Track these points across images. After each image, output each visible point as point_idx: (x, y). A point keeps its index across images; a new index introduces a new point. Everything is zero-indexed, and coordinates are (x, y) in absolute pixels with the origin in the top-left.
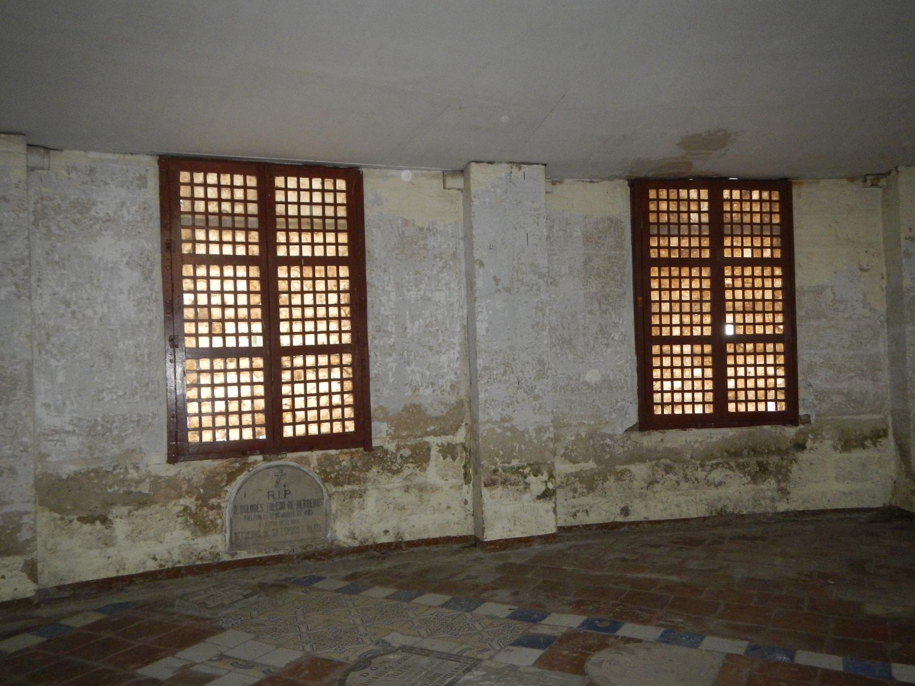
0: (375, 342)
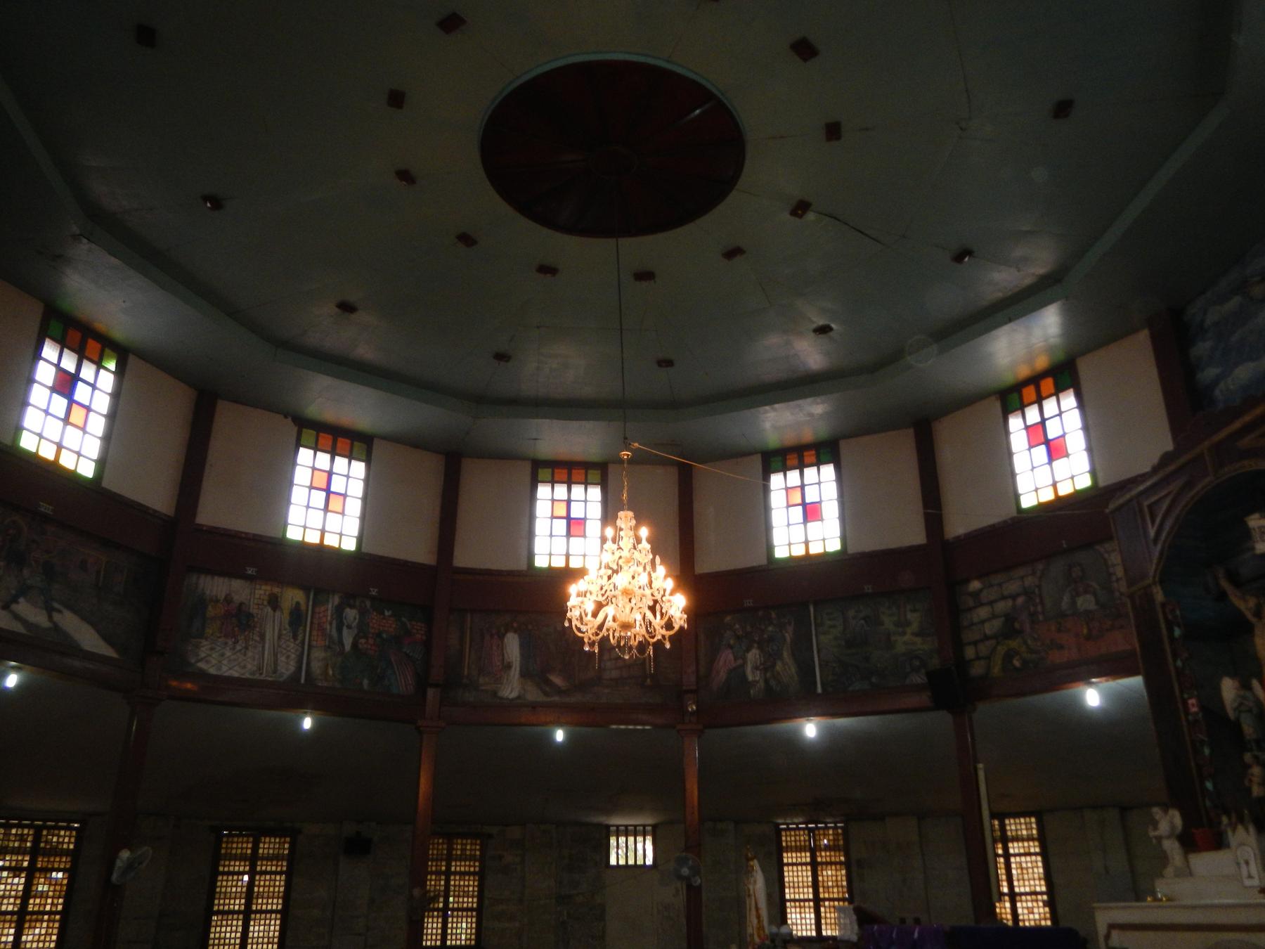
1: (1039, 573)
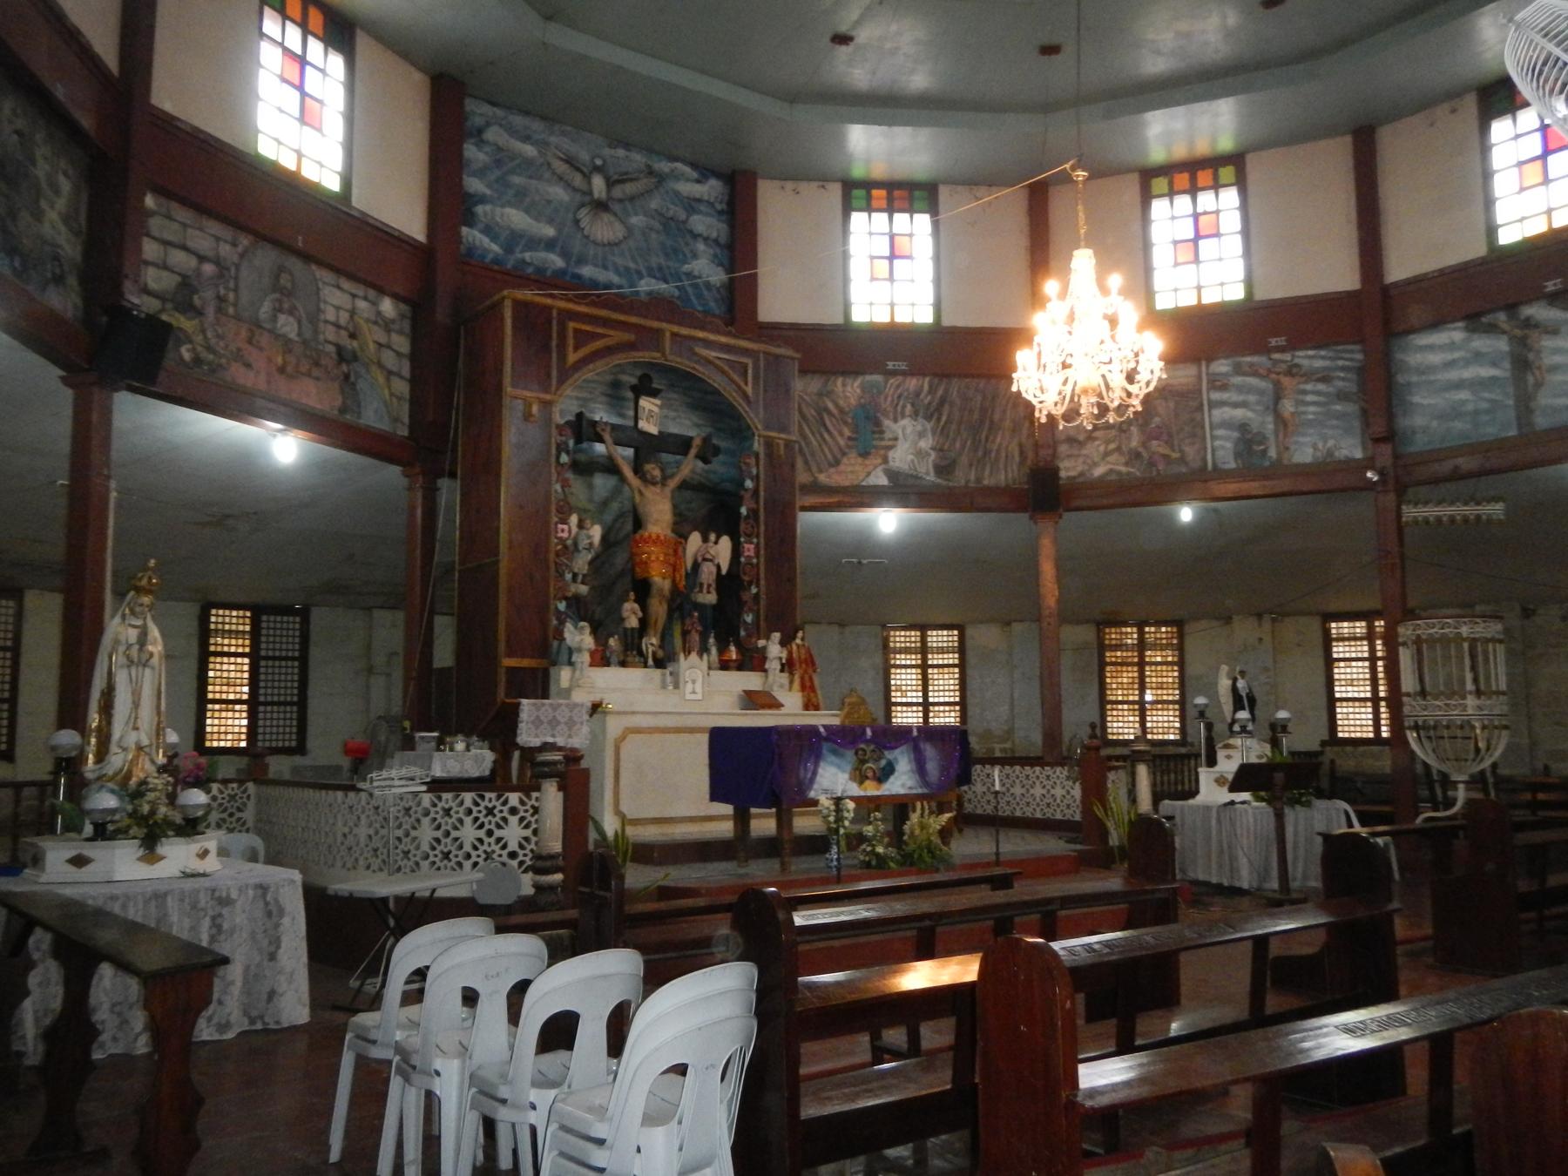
0: (970, 700)
1: (240, 249)
